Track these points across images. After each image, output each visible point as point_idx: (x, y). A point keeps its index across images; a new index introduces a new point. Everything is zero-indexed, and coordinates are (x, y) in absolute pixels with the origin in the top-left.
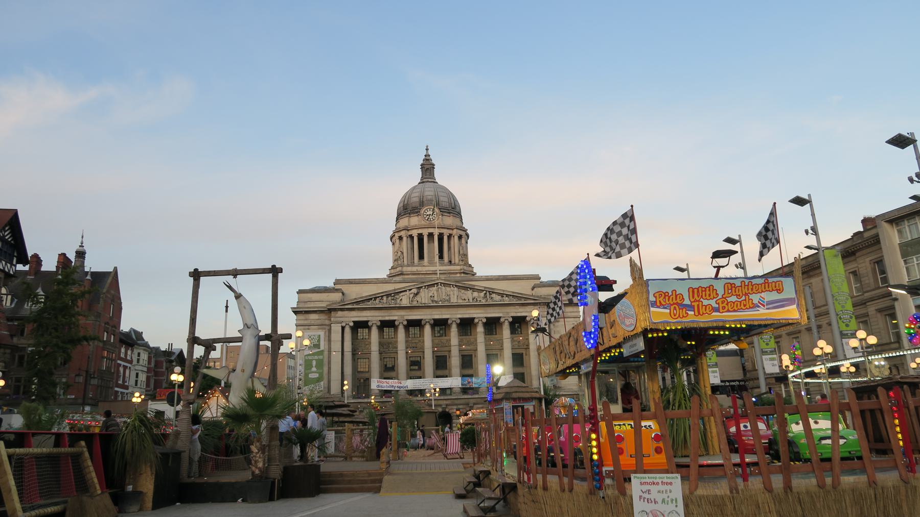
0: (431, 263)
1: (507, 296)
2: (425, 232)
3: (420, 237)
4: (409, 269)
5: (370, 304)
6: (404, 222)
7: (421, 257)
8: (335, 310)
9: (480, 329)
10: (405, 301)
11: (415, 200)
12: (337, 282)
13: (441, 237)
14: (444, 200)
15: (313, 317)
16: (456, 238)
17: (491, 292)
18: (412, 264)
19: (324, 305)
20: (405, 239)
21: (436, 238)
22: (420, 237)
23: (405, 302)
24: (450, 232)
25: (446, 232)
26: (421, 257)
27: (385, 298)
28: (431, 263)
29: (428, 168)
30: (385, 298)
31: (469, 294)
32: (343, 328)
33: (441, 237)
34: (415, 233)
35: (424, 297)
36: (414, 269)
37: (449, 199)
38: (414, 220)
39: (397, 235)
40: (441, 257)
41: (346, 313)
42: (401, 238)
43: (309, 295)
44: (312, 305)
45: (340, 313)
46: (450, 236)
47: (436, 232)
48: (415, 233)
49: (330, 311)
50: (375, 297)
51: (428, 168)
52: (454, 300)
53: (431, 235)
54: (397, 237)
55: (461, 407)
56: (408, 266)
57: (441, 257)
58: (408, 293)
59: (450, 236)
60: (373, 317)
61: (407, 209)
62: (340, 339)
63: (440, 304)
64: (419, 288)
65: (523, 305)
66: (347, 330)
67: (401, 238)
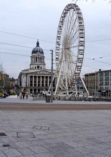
0: (38, 62)
2: (37, 57)
3: (37, 58)
5: (33, 73)
6: (34, 54)
7: (37, 61)
9: (49, 78)
11: (36, 50)
12: (28, 69)
13: (40, 58)
14: (41, 51)
15: (25, 74)
18: (35, 63)
21: (39, 58)
22: (37, 58)
23: (38, 73)
25: (41, 57)
26: (37, 61)
28: (38, 62)
29: (38, 44)
31: (47, 73)
32: (29, 77)
33: (40, 58)
35: (41, 73)
38: (36, 54)
40: (40, 61)
42: (33, 57)
43: (24, 71)
44: (24, 73)
47: (39, 57)
49: (27, 74)
50: (34, 72)
51: (38, 44)
52: (45, 73)
53: (38, 58)
54: (32, 57)
56: (34, 63)
57: (40, 61)
60: (34, 75)
61: (34, 52)
66: (30, 77)
67: (33, 57)
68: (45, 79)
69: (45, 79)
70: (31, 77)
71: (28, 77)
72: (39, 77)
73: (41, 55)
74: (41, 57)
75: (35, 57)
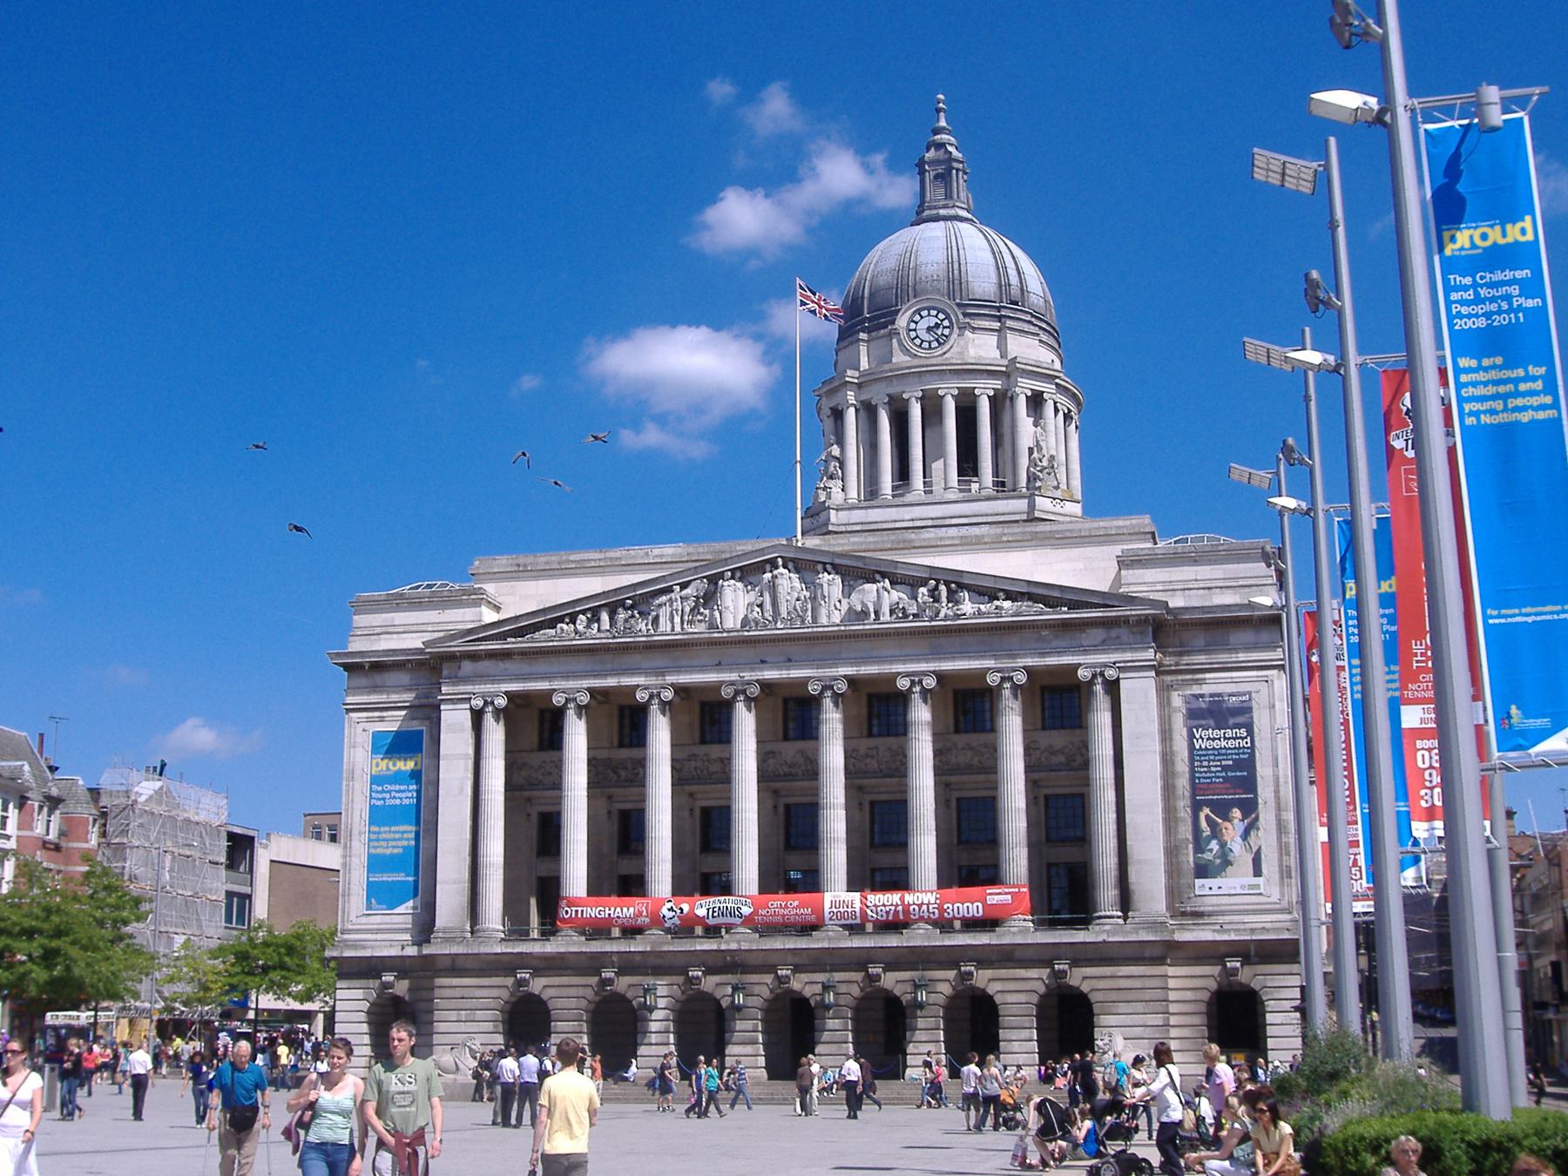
1: (1010, 596)
4: (858, 516)
7: (903, 473)
8: (452, 657)
10: (670, 622)
14: (983, 282)
16: (1021, 404)
17: (958, 584)
19: (414, 642)
20: (851, 414)
21: (950, 407)
24: (997, 384)
25: (985, 389)
26: (903, 473)
27: (605, 617)
30: (605, 617)
31: (880, 597)
32: (477, 717)
34: (878, 394)
36: (875, 515)
37: (1000, 268)
39: (826, 405)
41: (485, 666)
42: (838, 415)
45: (467, 667)
46: (1000, 402)
48: (878, 394)
52: (832, 616)
55: (838, 976)
58: (676, 594)
59: (1000, 402)
62: (471, 751)
63: (781, 629)
64: (714, 580)
65: (1065, 625)
68: (833, 756)
69: (833, 756)
70: (535, 728)
71: (455, 720)
72: (706, 719)
73: (980, 347)
74: (985, 389)
75: (868, 411)
